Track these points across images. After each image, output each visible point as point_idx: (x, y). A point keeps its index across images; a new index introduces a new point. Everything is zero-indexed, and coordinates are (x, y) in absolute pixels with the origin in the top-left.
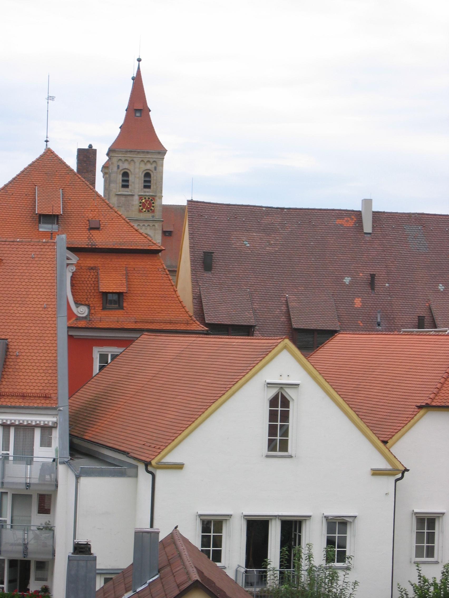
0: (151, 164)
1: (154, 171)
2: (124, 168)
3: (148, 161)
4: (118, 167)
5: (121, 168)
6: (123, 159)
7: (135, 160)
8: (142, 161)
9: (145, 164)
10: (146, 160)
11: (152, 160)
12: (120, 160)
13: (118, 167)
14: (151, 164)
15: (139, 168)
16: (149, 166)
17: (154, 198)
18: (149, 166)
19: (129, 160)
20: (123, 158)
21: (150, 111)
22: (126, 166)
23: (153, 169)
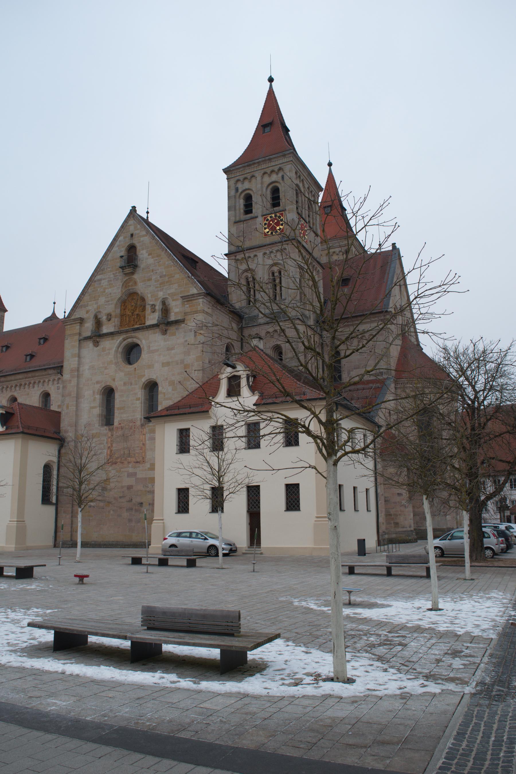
0: (277, 174)
1: (281, 182)
2: (244, 188)
3: (273, 171)
4: (237, 190)
5: (240, 191)
6: (241, 178)
7: (257, 174)
8: (265, 173)
9: (270, 176)
10: (268, 171)
11: (276, 169)
12: (238, 181)
13: (237, 190)
14: (277, 174)
15: (262, 183)
16: (274, 177)
17: (282, 214)
18: (274, 177)
19: (249, 177)
20: (240, 177)
21: (289, 131)
22: (246, 185)
23: (281, 179)
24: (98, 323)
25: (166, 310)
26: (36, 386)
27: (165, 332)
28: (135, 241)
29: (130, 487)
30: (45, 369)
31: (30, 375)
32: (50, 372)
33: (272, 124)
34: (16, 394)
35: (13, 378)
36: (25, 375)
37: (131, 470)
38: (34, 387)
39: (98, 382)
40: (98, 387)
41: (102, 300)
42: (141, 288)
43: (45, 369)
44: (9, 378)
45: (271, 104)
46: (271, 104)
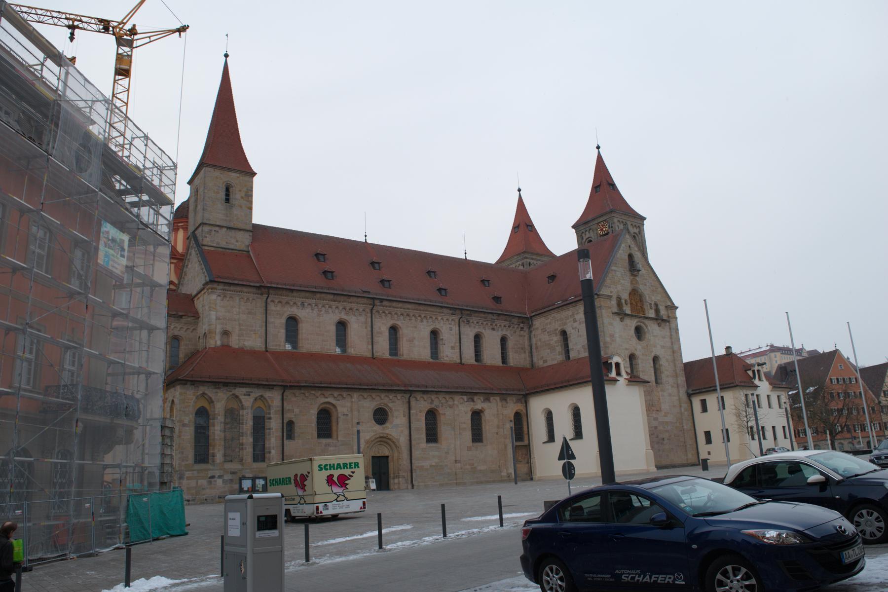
24: (619, 304)
25: (657, 311)
26: (425, 320)
27: (659, 325)
28: (633, 252)
29: (656, 428)
30: (442, 307)
31: (422, 308)
32: (445, 311)
33: (603, 182)
34: (399, 323)
35: (400, 305)
36: (417, 307)
37: (655, 416)
38: (422, 321)
39: (626, 349)
40: (628, 353)
41: (619, 287)
42: (642, 288)
43: (442, 307)
44: (395, 304)
45: (601, 168)
46: (601, 168)
